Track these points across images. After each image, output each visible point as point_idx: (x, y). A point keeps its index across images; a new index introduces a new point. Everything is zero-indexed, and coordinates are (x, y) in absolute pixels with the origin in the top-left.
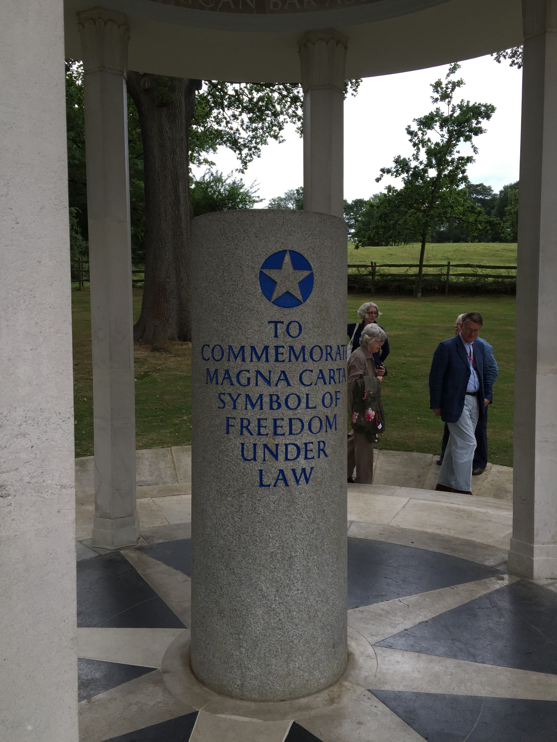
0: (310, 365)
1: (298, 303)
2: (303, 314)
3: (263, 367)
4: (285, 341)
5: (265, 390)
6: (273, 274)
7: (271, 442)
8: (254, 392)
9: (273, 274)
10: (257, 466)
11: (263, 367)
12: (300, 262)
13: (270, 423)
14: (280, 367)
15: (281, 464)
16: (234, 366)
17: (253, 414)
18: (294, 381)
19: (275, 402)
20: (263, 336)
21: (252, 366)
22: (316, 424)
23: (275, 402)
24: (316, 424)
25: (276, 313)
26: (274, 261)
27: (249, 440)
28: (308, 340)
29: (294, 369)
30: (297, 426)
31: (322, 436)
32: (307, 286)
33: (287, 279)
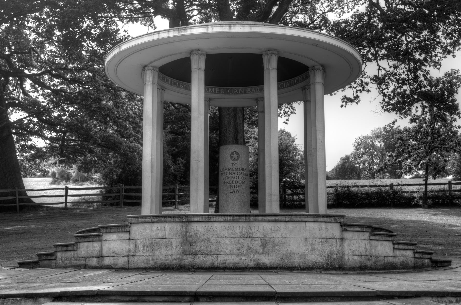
0: (239, 171)
1: (237, 160)
2: (238, 162)
3: (231, 171)
4: (234, 167)
5: (231, 175)
6: (232, 155)
7: (232, 185)
8: (229, 176)
9: (232, 155)
10: (229, 189)
11: (231, 171)
12: (237, 153)
13: (231, 181)
14: (233, 172)
15: (234, 189)
16: (226, 172)
17: (229, 180)
18: (236, 174)
19: (233, 178)
20: (230, 166)
21: (228, 171)
22: (240, 182)
23: (233, 178)
24: (240, 182)
25: (232, 162)
26: (232, 153)
27: (228, 185)
28: (239, 167)
29: (236, 172)
30: (236, 182)
31: (242, 184)
32: (238, 157)
33: (235, 156)
